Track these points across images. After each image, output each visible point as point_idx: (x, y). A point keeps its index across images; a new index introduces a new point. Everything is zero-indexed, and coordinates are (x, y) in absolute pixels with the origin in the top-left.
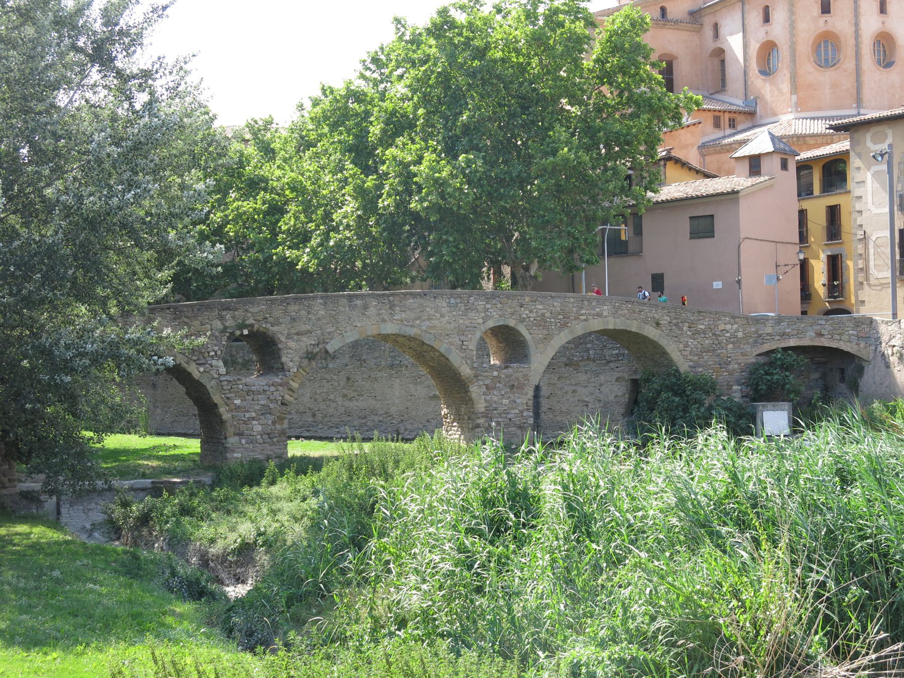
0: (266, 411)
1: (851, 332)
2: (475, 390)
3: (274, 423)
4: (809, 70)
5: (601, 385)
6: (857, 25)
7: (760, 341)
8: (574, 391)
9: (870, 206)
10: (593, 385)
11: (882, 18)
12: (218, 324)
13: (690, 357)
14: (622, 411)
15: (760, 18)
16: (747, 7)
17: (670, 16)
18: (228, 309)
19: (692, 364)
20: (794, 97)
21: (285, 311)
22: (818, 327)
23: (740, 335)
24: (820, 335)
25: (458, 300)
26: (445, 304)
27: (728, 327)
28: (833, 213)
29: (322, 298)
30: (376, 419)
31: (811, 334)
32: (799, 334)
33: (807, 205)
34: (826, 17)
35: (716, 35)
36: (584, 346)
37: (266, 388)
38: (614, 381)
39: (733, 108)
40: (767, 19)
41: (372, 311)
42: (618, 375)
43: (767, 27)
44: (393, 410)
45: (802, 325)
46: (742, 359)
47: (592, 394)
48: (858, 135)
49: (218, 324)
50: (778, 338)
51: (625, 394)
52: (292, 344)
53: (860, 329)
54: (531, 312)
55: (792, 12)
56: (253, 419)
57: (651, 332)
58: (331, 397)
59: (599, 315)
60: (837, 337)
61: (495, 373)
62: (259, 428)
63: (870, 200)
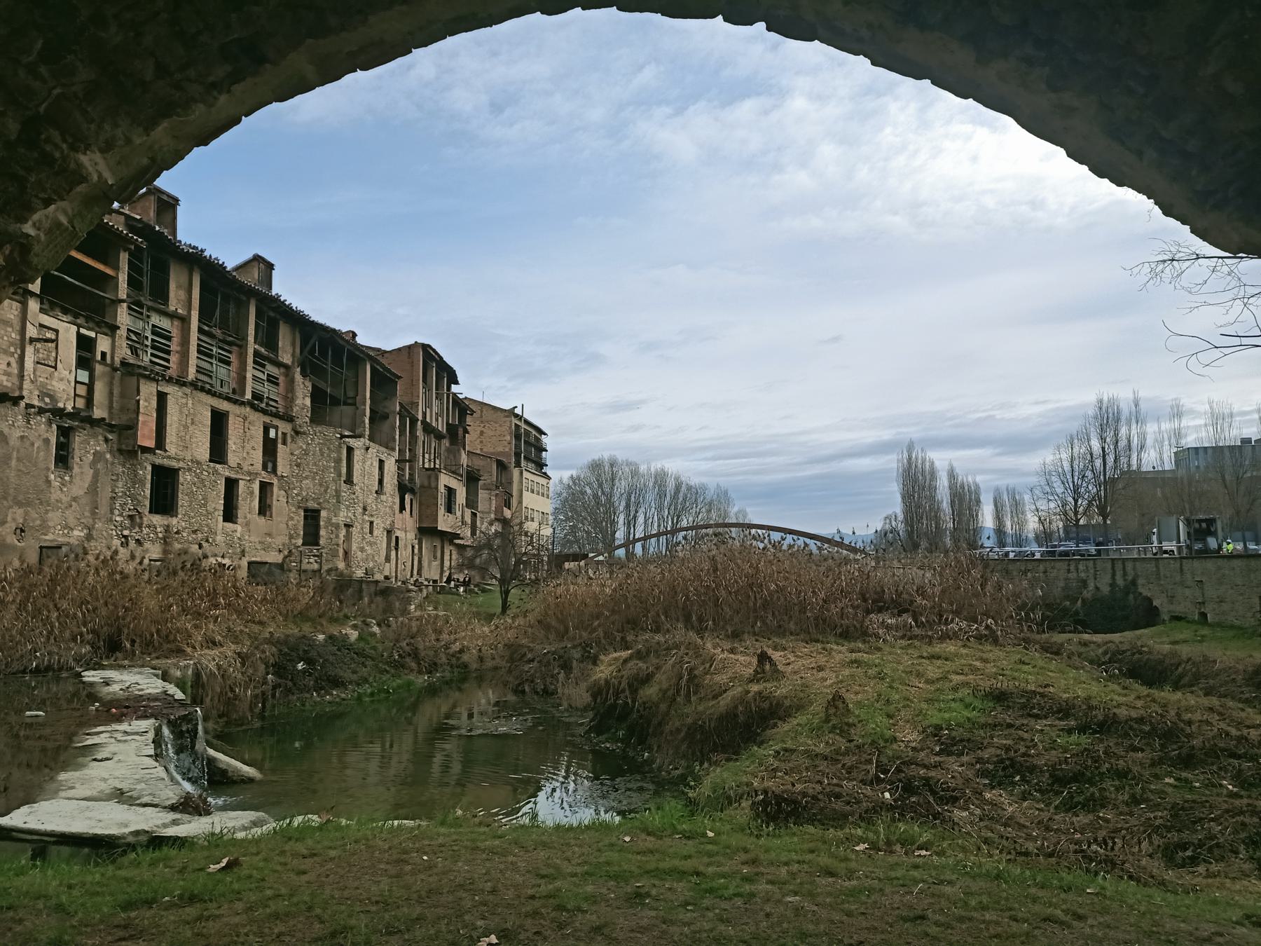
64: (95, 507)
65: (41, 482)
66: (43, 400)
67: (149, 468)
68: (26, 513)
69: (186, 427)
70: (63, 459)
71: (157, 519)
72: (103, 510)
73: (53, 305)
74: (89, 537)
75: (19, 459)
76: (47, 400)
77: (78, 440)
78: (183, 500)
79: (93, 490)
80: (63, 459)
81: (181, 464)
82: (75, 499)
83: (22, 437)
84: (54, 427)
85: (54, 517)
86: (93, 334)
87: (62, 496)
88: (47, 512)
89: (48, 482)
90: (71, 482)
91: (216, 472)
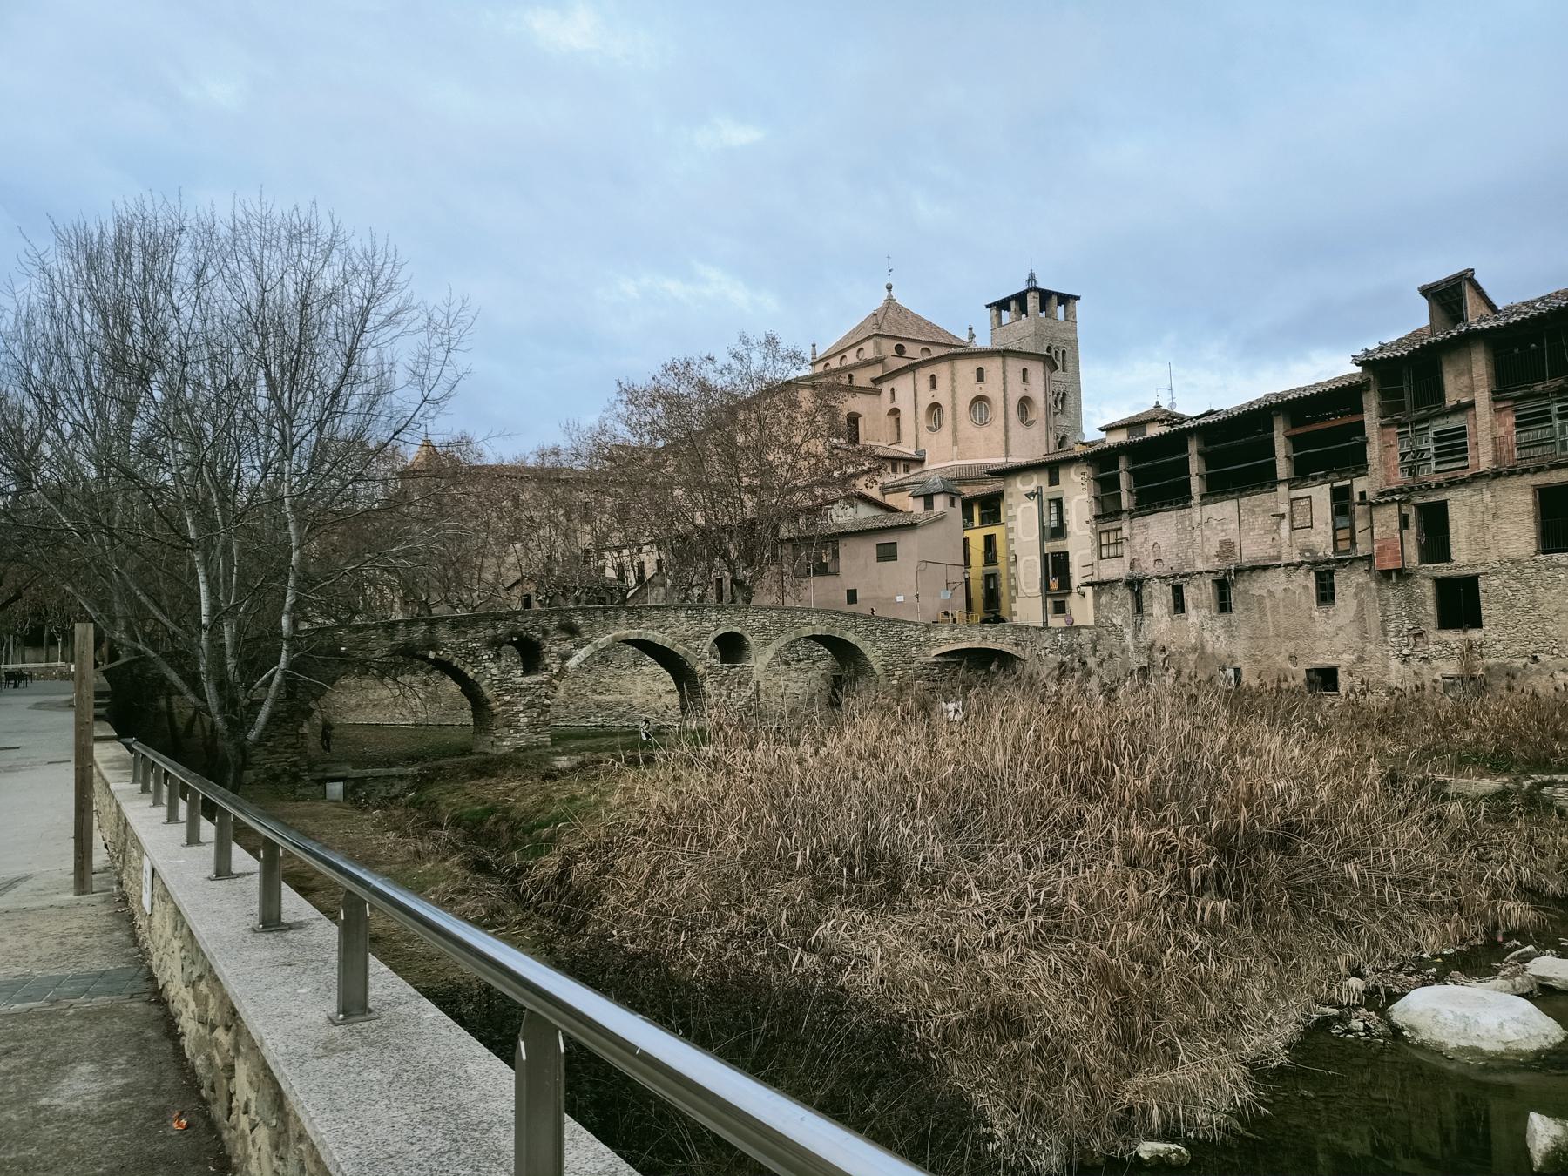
0: (531, 705)
2: (708, 687)
3: (539, 715)
4: (965, 424)
6: (1005, 391)
8: (787, 686)
9: (1021, 536)
11: (1024, 386)
12: (490, 632)
13: (882, 658)
15: (928, 384)
16: (917, 376)
18: (500, 619)
20: (956, 448)
21: (550, 620)
23: (922, 639)
24: (985, 639)
25: (694, 612)
26: (683, 615)
27: (912, 633)
28: (989, 541)
29: (581, 609)
30: (621, 709)
32: (970, 638)
33: (967, 534)
34: (981, 385)
35: (893, 399)
37: (532, 686)
39: (908, 456)
40: (933, 386)
41: (623, 620)
42: (822, 672)
43: (933, 392)
44: (635, 702)
46: (923, 659)
48: (1009, 480)
49: (490, 632)
52: (555, 649)
54: (754, 621)
55: (953, 380)
56: (521, 712)
57: (851, 638)
58: (583, 692)
59: (810, 624)
61: (725, 672)
62: (526, 720)
63: (1020, 532)
64: (1363, 636)
65: (1306, 620)
66: (1304, 555)
67: (1429, 584)
68: (1298, 645)
69: (1484, 525)
70: (1326, 595)
71: (1453, 637)
72: (1374, 632)
73: (1304, 480)
74: (1361, 659)
75: (1285, 606)
76: (1307, 554)
77: (1338, 579)
78: (1488, 609)
79: (1360, 617)
80: (1326, 595)
81: (1479, 570)
82: (1340, 628)
83: (1285, 589)
84: (1312, 574)
85: (1322, 645)
86: (1348, 482)
87: (1328, 628)
88: (1314, 642)
89: (1311, 618)
90: (1335, 615)
91: (1555, 566)
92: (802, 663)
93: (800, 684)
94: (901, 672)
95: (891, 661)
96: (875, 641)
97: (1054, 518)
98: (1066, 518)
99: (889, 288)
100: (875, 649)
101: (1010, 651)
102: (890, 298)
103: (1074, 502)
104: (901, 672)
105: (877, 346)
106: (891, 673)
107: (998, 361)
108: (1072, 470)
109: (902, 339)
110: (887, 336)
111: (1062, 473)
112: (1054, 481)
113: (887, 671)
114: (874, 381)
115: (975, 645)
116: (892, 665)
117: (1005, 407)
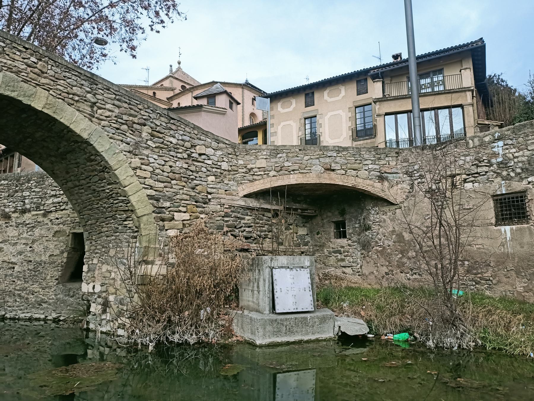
1: (370, 166)
5: (33, 242)
7: (251, 178)
10: (24, 241)
11: (253, 107)
14: (57, 274)
17: (157, 97)
19: (152, 192)
22: (327, 160)
23: (225, 166)
27: (210, 151)
31: (320, 168)
32: (303, 169)
36: (20, 194)
38: (50, 236)
42: (56, 228)
45: (306, 158)
46: (227, 200)
47: (20, 253)
50: (272, 173)
51: (62, 252)
53: (383, 162)
60: (354, 173)
92: (27, 215)
93: (19, 247)
94: (186, 216)
95: (168, 191)
96: (137, 145)
97: (308, 131)
98: (319, 131)
99: (179, 63)
100: (136, 161)
101: (369, 189)
102: (179, 68)
103: (327, 118)
104: (186, 216)
105: (171, 82)
106: (167, 215)
107: (240, 90)
108: (326, 93)
109: (185, 83)
110: (177, 79)
111: (317, 96)
112: (309, 103)
113: (159, 210)
114: (168, 99)
115: (311, 179)
116: (170, 199)
117: (243, 115)
